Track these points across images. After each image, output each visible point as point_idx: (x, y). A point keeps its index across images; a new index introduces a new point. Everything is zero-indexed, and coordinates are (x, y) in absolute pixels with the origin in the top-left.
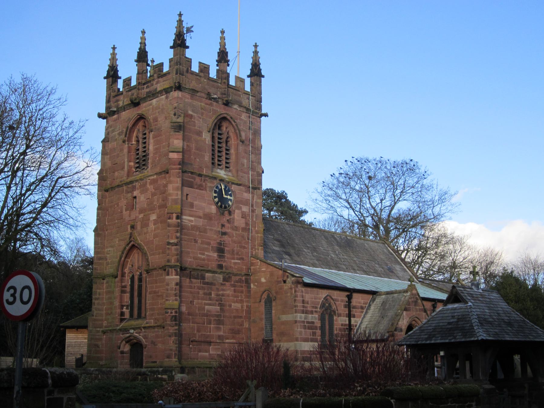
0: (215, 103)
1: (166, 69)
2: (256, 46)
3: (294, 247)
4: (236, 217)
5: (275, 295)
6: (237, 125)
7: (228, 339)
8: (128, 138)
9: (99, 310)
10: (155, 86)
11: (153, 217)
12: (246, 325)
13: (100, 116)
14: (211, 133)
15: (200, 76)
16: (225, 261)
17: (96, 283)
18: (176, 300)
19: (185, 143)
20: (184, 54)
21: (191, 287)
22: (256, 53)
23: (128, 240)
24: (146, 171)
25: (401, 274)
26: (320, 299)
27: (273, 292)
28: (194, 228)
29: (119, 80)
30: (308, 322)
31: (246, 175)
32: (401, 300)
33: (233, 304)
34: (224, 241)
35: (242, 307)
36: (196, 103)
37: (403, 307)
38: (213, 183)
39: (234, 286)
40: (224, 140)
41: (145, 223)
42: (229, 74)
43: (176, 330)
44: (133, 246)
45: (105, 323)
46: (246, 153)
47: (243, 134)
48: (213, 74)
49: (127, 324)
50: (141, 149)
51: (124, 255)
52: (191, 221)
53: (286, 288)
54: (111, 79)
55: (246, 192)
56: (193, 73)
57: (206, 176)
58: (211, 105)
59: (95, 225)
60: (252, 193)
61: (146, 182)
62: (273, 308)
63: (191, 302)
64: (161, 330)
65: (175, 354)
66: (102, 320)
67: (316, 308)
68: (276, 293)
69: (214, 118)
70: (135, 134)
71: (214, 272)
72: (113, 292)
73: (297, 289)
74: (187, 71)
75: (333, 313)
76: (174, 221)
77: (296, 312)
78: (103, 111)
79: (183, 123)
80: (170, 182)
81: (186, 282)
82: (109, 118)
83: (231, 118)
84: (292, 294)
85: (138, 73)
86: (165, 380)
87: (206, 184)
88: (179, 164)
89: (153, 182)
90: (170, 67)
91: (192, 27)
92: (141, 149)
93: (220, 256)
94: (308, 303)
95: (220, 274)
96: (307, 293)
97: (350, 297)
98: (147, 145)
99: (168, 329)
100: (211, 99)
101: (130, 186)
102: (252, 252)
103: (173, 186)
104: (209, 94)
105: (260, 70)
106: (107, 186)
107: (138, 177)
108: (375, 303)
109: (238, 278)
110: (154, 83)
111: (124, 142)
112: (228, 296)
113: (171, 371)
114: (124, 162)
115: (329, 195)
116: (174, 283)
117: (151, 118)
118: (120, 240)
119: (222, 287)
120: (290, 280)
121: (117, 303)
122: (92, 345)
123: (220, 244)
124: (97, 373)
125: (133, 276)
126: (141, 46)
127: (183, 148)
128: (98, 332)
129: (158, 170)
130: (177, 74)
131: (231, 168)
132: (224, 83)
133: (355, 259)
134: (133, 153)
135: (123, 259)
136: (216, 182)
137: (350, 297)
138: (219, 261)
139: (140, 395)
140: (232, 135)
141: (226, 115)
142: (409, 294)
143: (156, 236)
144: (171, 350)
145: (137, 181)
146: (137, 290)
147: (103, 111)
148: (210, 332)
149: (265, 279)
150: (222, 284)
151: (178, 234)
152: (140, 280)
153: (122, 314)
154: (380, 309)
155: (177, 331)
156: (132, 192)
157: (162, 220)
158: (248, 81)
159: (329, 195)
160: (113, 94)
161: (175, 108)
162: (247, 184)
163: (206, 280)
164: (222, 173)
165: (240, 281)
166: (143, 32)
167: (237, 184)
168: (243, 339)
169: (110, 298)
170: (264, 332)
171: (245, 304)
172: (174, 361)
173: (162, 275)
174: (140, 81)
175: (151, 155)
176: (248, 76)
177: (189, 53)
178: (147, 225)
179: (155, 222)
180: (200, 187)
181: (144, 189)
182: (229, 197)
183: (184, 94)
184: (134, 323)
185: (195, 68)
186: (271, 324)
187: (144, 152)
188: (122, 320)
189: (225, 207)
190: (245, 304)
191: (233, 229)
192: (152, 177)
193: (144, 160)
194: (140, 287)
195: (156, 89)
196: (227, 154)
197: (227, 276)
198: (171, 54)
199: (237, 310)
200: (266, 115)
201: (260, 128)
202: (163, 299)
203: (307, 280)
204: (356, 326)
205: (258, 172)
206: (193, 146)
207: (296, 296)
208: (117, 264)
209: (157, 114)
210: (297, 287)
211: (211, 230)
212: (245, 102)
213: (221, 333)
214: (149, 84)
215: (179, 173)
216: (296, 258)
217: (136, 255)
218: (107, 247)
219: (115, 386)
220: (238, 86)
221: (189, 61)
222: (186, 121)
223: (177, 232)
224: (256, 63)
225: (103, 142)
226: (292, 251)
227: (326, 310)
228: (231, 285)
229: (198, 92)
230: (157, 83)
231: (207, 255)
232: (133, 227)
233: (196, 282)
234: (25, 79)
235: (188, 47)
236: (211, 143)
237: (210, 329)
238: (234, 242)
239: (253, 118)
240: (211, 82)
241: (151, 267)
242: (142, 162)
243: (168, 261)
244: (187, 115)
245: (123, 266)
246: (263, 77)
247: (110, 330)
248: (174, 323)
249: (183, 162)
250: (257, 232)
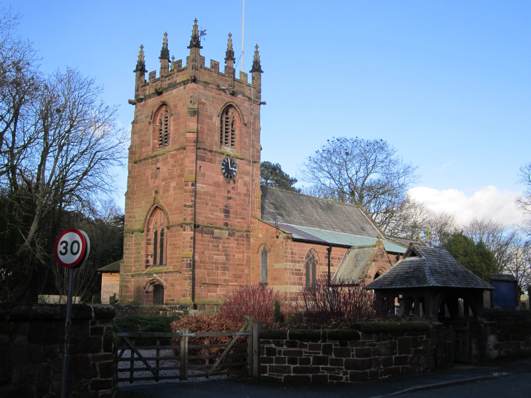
0: (223, 93)
1: (184, 65)
2: (257, 47)
3: (285, 210)
4: (239, 185)
5: (269, 247)
6: (241, 112)
7: (232, 282)
8: (153, 120)
9: (129, 258)
10: (175, 79)
11: (173, 184)
12: (246, 271)
13: (131, 102)
14: (220, 117)
15: (212, 72)
16: (230, 220)
17: (127, 237)
18: (191, 251)
19: (199, 125)
21: (202, 241)
22: (257, 52)
23: (152, 202)
24: (167, 148)
25: (371, 232)
26: (305, 251)
27: (268, 245)
28: (206, 193)
29: (146, 73)
30: (296, 270)
31: (248, 152)
32: (370, 253)
33: (236, 255)
35: (243, 257)
36: (207, 93)
37: (372, 259)
38: (221, 158)
39: (237, 240)
40: (230, 123)
41: (166, 191)
42: (234, 70)
44: (157, 207)
45: (133, 269)
46: (247, 133)
47: (246, 119)
48: (222, 70)
49: (151, 269)
50: (164, 130)
51: (149, 214)
52: (204, 188)
53: (278, 242)
54: (139, 72)
55: (248, 165)
56: (206, 69)
57: (216, 152)
58: (220, 94)
59: (126, 190)
60: (253, 166)
61: (168, 156)
62: (268, 258)
63: (203, 252)
64: (178, 275)
65: (190, 294)
66: (131, 266)
67: (302, 258)
68: (271, 246)
69: (222, 105)
70: (158, 117)
71: (221, 229)
72: (140, 244)
73: (287, 243)
74: (201, 67)
75: (315, 263)
76: (190, 187)
77: (286, 262)
78: (133, 98)
79: (198, 109)
80: (187, 156)
81: (199, 236)
82: (138, 104)
84: (283, 247)
85: (162, 68)
86: (181, 314)
87: (215, 159)
88: (194, 142)
89: (173, 156)
90: (187, 63)
91: (205, 30)
92: (164, 130)
93: (226, 216)
94: (296, 254)
95: (226, 230)
96: (295, 246)
97: (329, 250)
98: (168, 126)
99: (184, 274)
100: (220, 90)
101: (155, 159)
102: (252, 213)
103: (189, 159)
104: (218, 86)
105: (260, 67)
106: (136, 159)
107: (161, 152)
108: (350, 254)
109: (240, 234)
110: (175, 76)
111: (150, 123)
112: (232, 248)
113: (186, 308)
114: (150, 140)
115: (314, 168)
116: (189, 237)
117: (171, 104)
118: (146, 203)
119: (226, 241)
120: (282, 236)
121: (143, 253)
122: (123, 287)
124: (127, 308)
125: (156, 231)
127: (197, 130)
128: (128, 275)
129: (177, 146)
130: (193, 69)
131: (236, 146)
132: (231, 77)
133: (334, 220)
134: (157, 133)
135: (148, 217)
136: (223, 157)
137: (329, 250)
139: (162, 326)
140: (236, 119)
141: (232, 103)
142: (377, 248)
143: (175, 200)
144: (186, 291)
145: (160, 155)
146: (159, 244)
147: (133, 98)
149: (262, 235)
150: (227, 239)
151: (193, 199)
152: (162, 235)
153: (147, 261)
154: (353, 260)
155: (191, 276)
156: (156, 164)
157: (179, 187)
158: (250, 76)
159: (314, 168)
160: (141, 85)
161: (191, 97)
162: (248, 158)
163: (215, 235)
164: (228, 149)
165: (242, 236)
166: (166, 35)
167: (240, 159)
168: (244, 282)
169: (138, 249)
170: (261, 277)
171: (246, 255)
172: (188, 300)
173: (180, 230)
174: (163, 74)
175: (171, 135)
176: (250, 72)
177: (202, 52)
178: (168, 191)
179: (175, 189)
180: (211, 161)
181: (165, 163)
182: (234, 169)
183: (198, 85)
184: (157, 269)
185: (208, 65)
187: (166, 132)
188: (147, 266)
189: (231, 177)
190: (246, 255)
191: (237, 195)
192: (172, 153)
193: (166, 139)
194: (162, 240)
195: (176, 81)
196: (232, 134)
197: (232, 232)
198: (188, 52)
199: (239, 259)
200: (264, 103)
201: (259, 114)
202: (180, 249)
203: (295, 236)
204: (334, 273)
205: (257, 149)
206: (205, 127)
207: (287, 249)
208: (143, 222)
209: (177, 102)
210: (287, 241)
211: (219, 195)
212: (247, 93)
213: (227, 278)
214: (170, 77)
215: (194, 149)
216: (288, 219)
217: (159, 214)
218: (136, 208)
219: (142, 319)
220: (242, 79)
221: (203, 59)
222: (199, 107)
223: (192, 196)
224: (256, 61)
225: (133, 123)
226: (284, 213)
227: (310, 260)
228: (235, 239)
229: (209, 84)
230: (177, 76)
231: (216, 215)
232: (156, 192)
233: (207, 237)
234: (69, 71)
235: (202, 48)
236: (220, 125)
238: (238, 205)
240: (220, 76)
241: (170, 225)
242: (164, 140)
243: (185, 220)
244: (200, 103)
245: (149, 223)
246: (263, 72)
247: (138, 274)
248: (189, 269)
249: (197, 140)
250: (256, 197)
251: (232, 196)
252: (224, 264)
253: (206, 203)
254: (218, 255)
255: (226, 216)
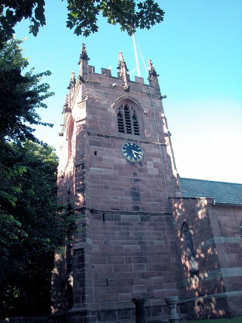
21: (104, 228)
34: (137, 186)
35: (166, 243)
83: (133, 99)
93: (135, 199)
109: (156, 217)
112: (149, 234)
119: (141, 226)
148: (131, 271)
164: (133, 136)
165: (160, 219)
177: (90, 63)
180: (108, 146)
185: (98, 71)
200: (165, 97)
206: (99, 117)
213: (145, 271)
237: (131, 268)
239: (157, 101)
251: (140, 178)
252: (138, 254)
253: (105, 187)
254: (128, 244)
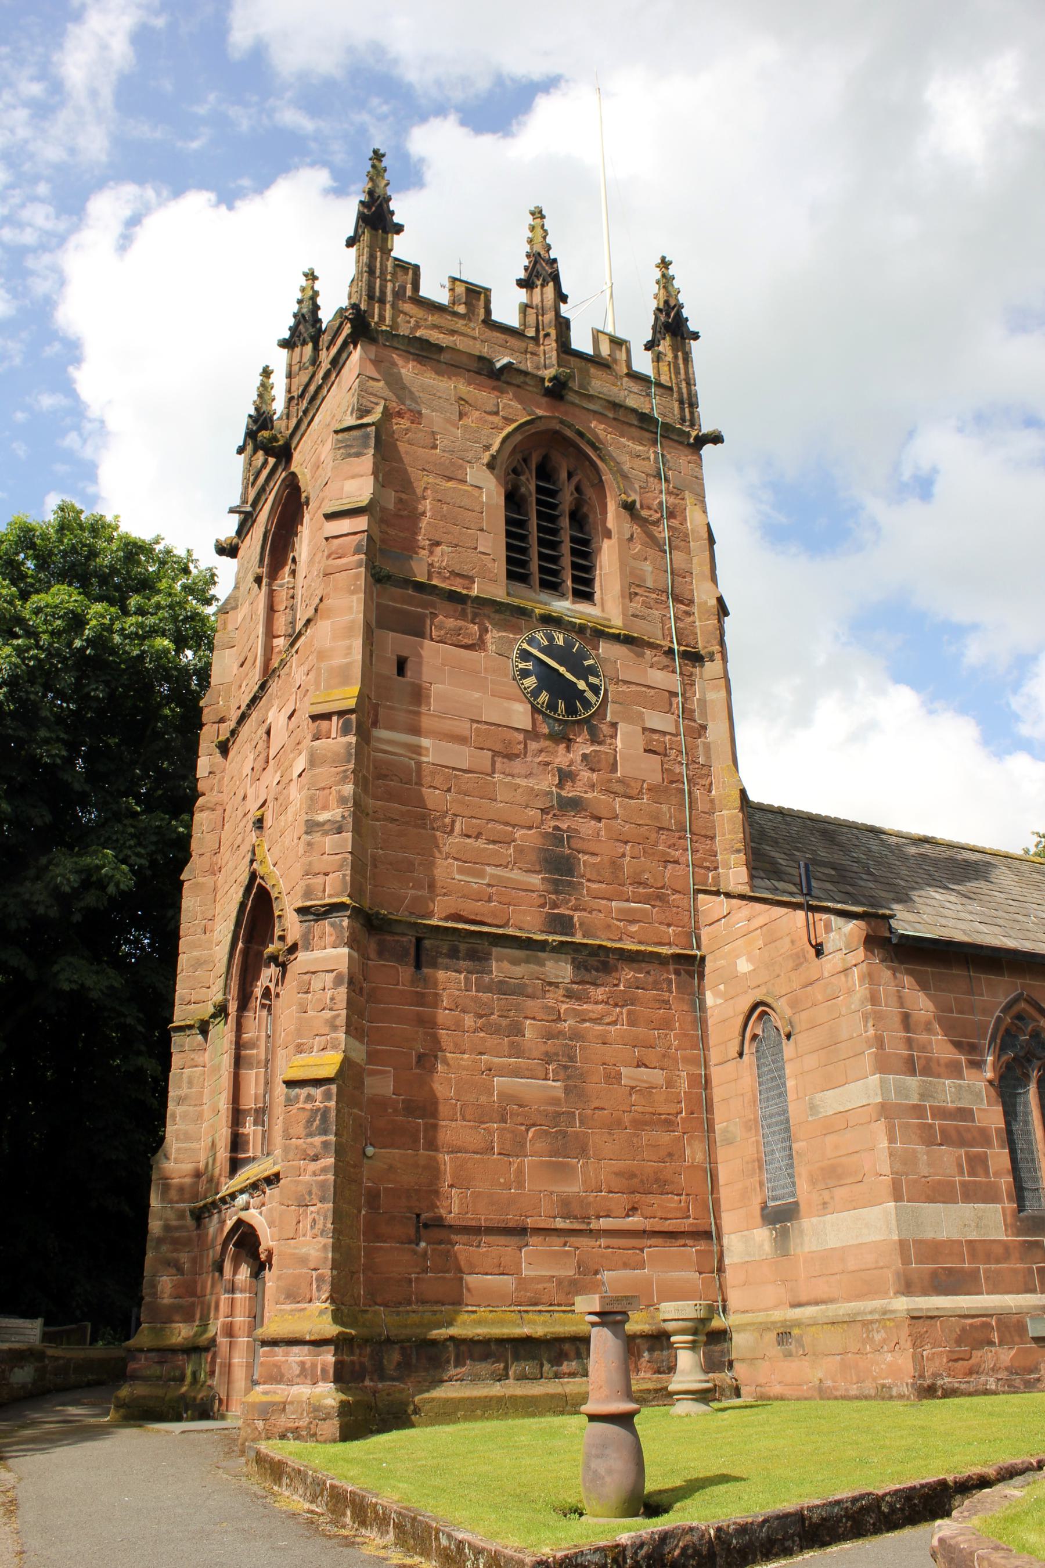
2: (665, 264)
20: (387, 251)
30: (941, 1113)
35: (670, 1084)
43: (324, 1170)
63: (420, 1057)
68: (794, 1004)
93: (557, 887)
111: (258, 580)
123: (557, 837)
126: (300, 309)
138: (555, 906)
148: (520, 1185)
149: (750, 960)
155: (331, 1177)
185: (434, 288)
186: (787, 1135)
200: (716, 439)
231: (492, 876)
235: (399, 229)
237: (520, 1172)
248: (318, 1140)
254: (516, 1073)
255: (556, 883)
